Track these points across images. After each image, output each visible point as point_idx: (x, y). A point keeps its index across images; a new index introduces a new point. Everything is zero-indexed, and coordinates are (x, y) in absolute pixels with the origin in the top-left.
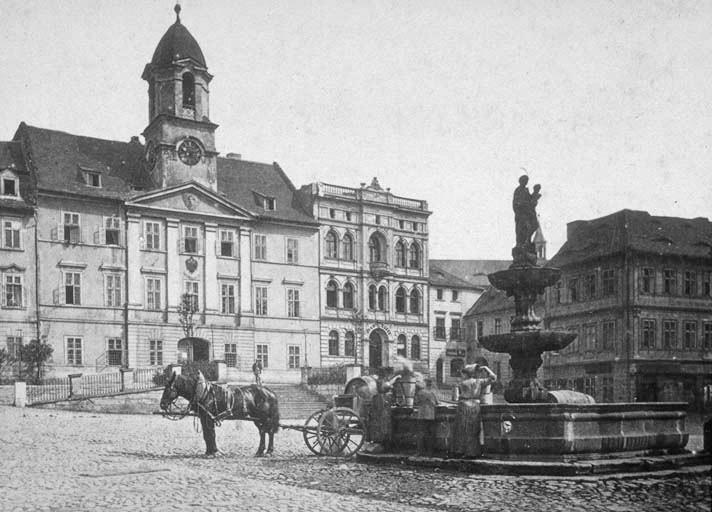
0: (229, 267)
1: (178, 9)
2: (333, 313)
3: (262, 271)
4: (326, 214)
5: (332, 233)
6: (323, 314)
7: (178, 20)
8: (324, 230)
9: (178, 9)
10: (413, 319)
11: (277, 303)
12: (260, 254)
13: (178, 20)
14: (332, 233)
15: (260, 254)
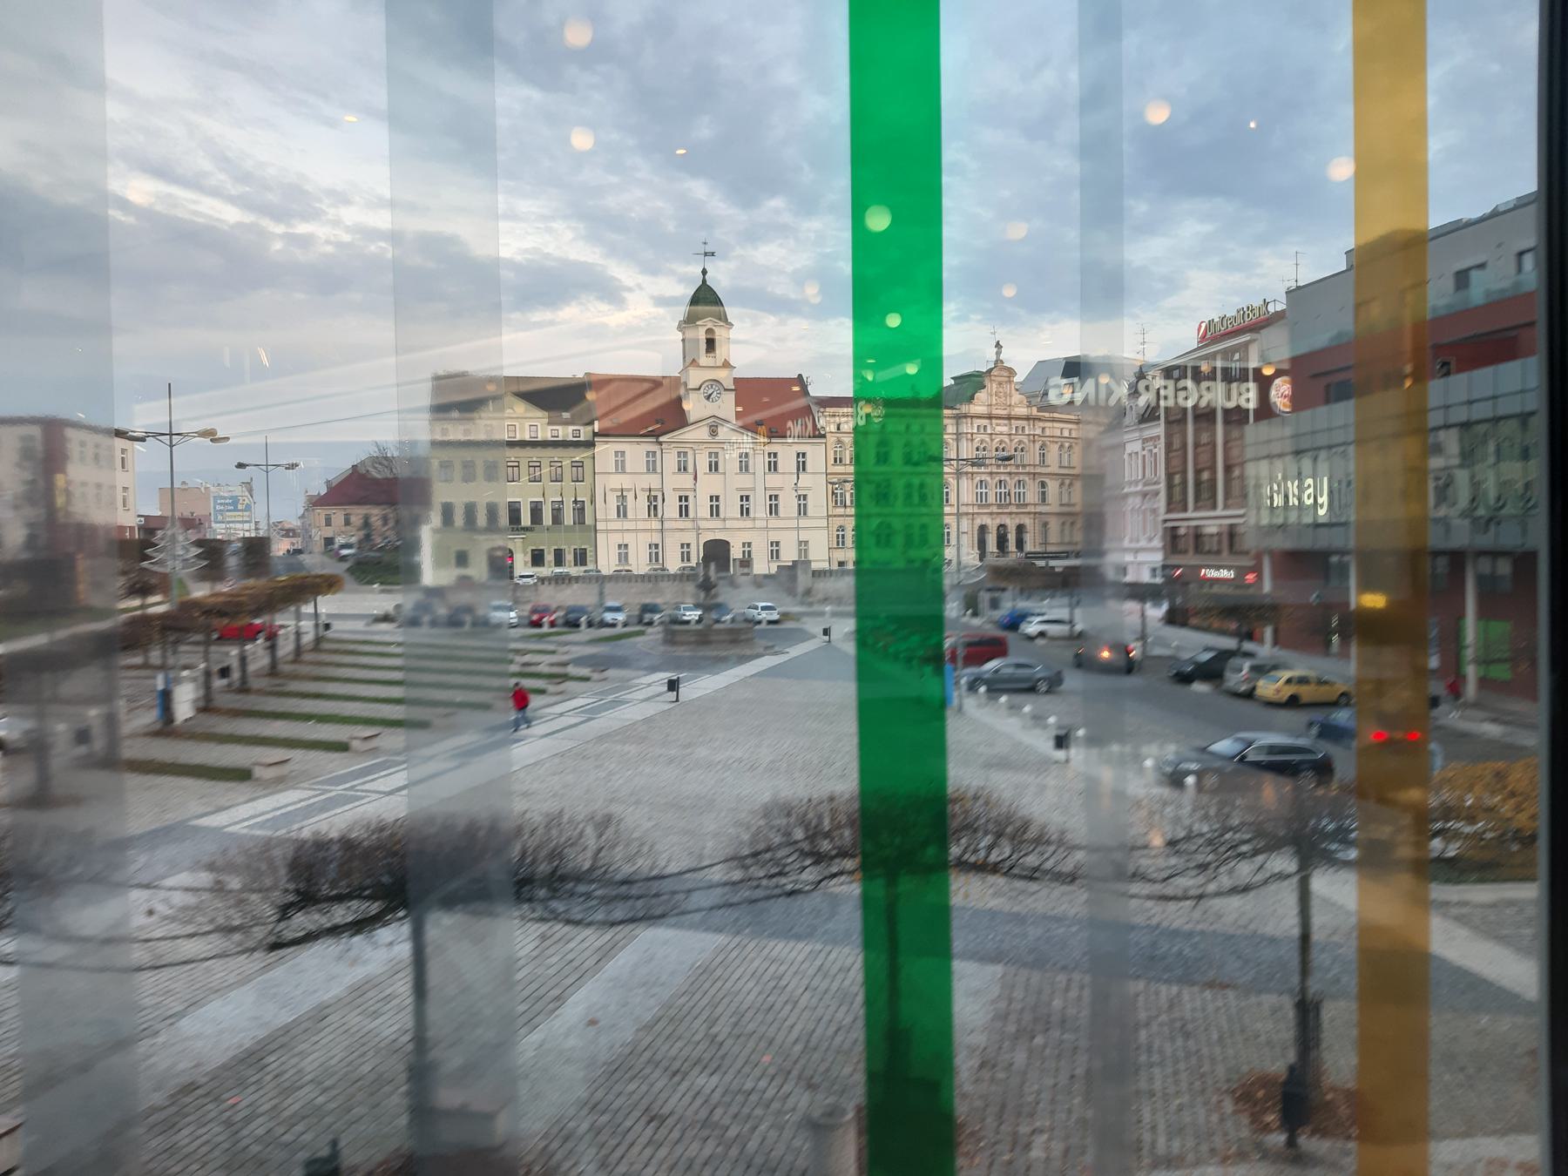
0: (745, 481)
1: (704, 272)
2: (841, 511)
3: (774, 480)
4: (833, 428)
5: (839, 441)
6: (830, 513)
7: (704, 281)
8: (831, 439)
9: (704, 272)
10: (924, 510)
11: (788, 505)
12: (773, 467)
13: (704, 281)
14: (839, 441)
15: (773, 467)
